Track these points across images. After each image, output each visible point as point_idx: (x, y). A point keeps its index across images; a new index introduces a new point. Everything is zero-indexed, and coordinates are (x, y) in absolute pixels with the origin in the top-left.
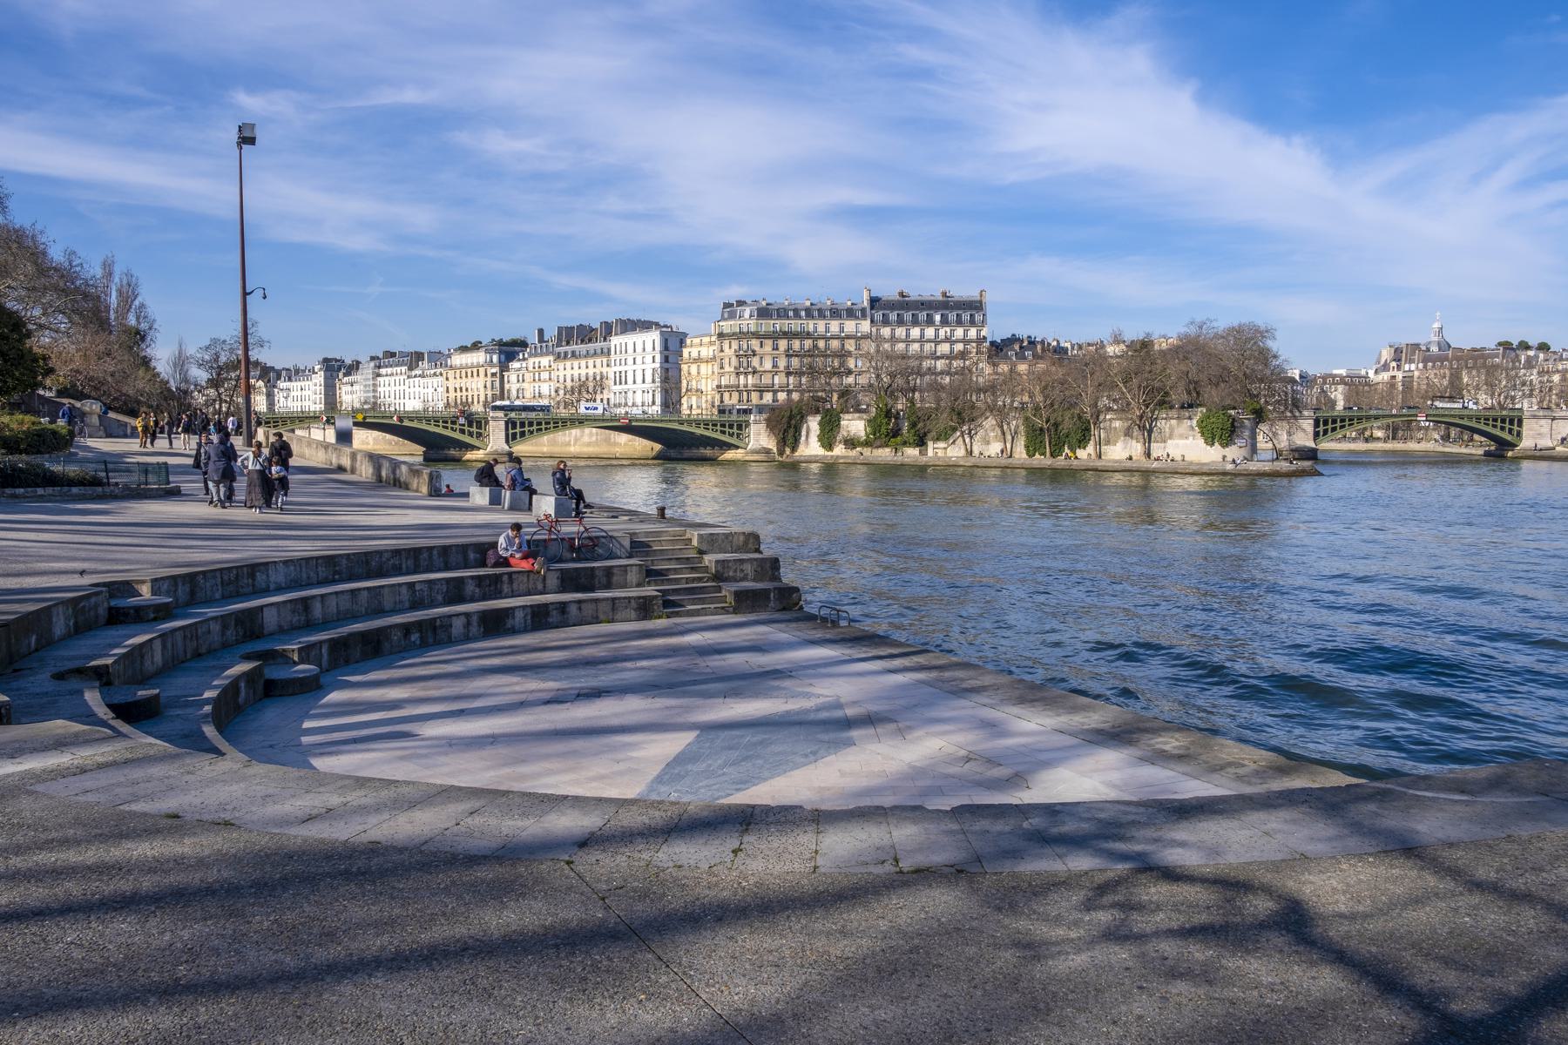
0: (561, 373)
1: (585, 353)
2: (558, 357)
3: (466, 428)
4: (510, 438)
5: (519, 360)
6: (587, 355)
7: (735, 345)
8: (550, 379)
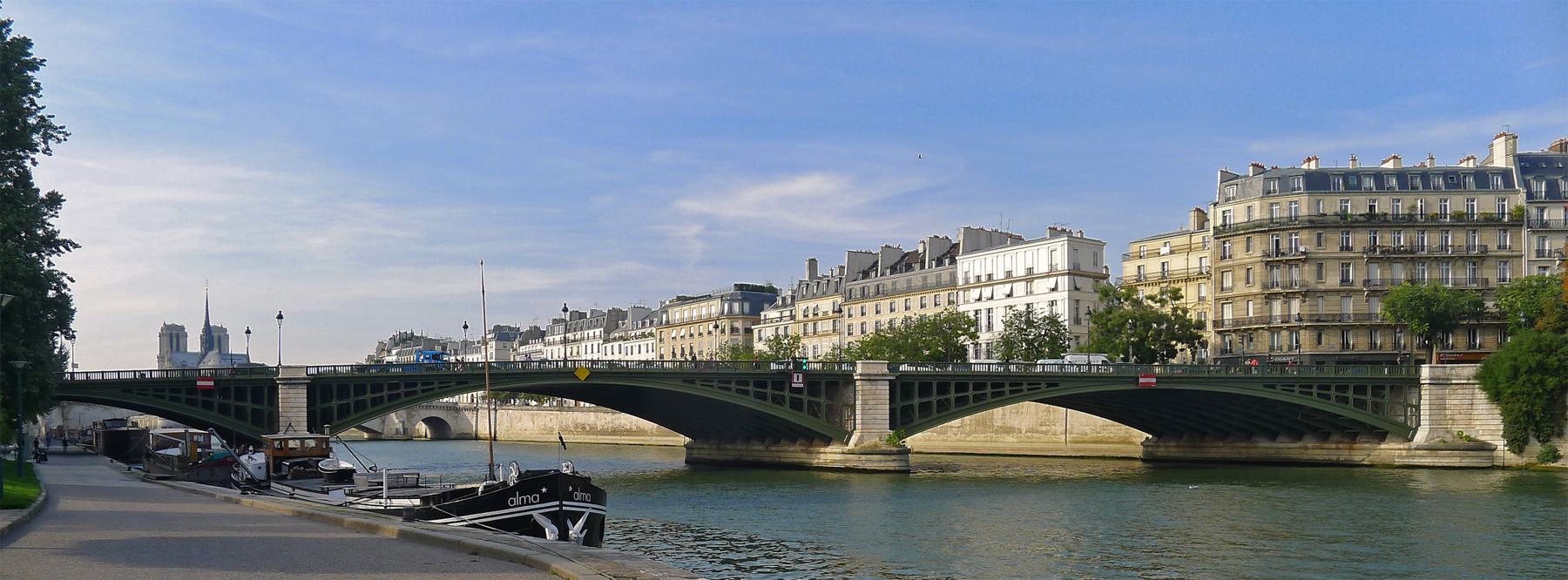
0: (856, 322)
1: (872, 290)
2: (849, 298)
3: (805, 397)
4: (904, 418)
5: (777, 307)
6: (909, 290)
7: (1260, 245)
8: (834, 331)
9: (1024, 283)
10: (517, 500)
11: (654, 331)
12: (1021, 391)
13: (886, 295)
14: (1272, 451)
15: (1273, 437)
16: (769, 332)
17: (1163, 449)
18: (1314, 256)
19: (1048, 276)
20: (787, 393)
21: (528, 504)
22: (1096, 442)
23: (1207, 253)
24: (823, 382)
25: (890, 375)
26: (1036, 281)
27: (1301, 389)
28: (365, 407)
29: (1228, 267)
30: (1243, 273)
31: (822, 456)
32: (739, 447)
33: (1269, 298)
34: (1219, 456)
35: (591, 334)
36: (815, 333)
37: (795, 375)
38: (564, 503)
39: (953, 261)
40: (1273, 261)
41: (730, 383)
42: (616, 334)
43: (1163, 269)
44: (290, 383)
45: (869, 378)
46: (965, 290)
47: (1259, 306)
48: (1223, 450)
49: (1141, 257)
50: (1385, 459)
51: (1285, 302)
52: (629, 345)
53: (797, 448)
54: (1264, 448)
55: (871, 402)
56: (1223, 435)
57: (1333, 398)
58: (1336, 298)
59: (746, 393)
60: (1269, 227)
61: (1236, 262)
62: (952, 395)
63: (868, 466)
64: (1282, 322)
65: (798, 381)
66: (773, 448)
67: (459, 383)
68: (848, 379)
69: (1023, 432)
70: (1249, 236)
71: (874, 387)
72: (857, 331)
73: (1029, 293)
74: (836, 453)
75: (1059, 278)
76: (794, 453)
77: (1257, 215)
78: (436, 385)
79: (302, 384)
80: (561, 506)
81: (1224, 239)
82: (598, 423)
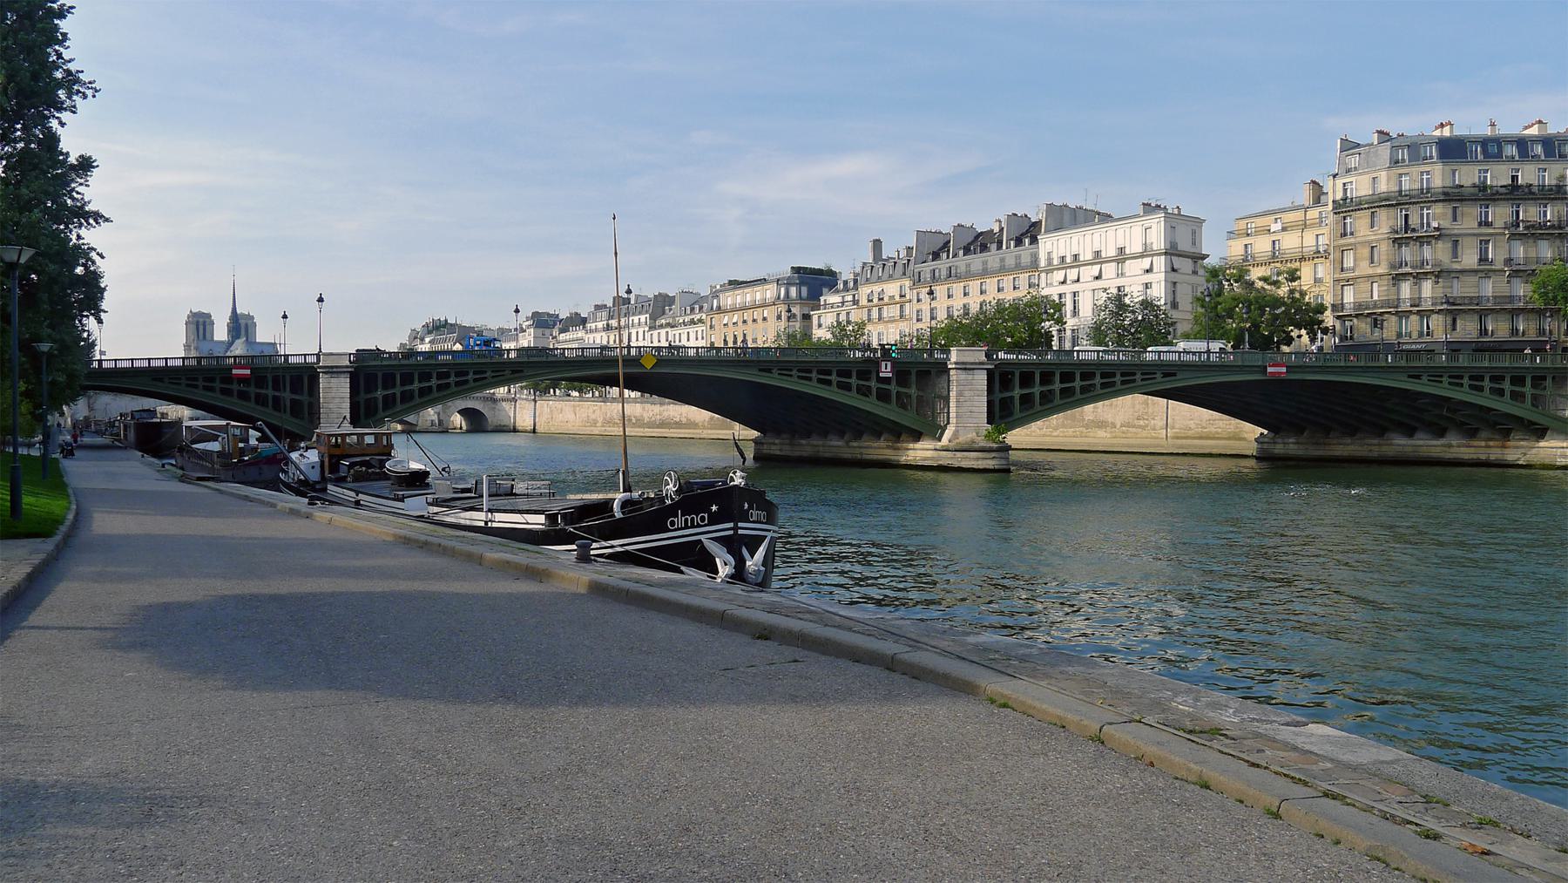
1: (944, 273)
4: (1002, 413)
5: (837, 291)
6: (985, 273)
7: (1387, 221)
8: (901, 316)
9: (1114, 264)
10: (680, 520)
11: (704, 317)
12: (1134, 381)
13: (959, 278)
14: (1410, 449)
15: (1410, 432)
16: (829, 319)
17: (1281, 446)
18: (1448, 232)
19: (1142, 256)
20: (873, 384)
21: (693, 526)
22: (1201, 438)
23: (1325, 230)
24: (914, 372)
25: (988, 364)
26: (1127, 262)
27: (1429, 378)
28: (412, 397)
29: (1348, 245)
30: (1366, 252)
31: (911, 453)
32: (815, 443)
33: (1397, 279)
34: (1346, 454)
35: (636, 321)
36: (880, 319)
37: (883, 364)
38: (740, 525)
39: (1034, 240)
40: (1403, 237)
41: (810, 372)
42: (663, 321)
43: (1274, 248)
44: (333, 371)
45: (964, 367)
46: (1047, 272)
47: (1386, 288)
48: (1351, 448)
49: (1248, 235)
50: (1543, 458)
51: (1415, 284)
52: (677, 333)
53: (882, 443)
54: (1399, 445)
55: (967, 393)
56: (1351, 431)
57: (1487, 390)
58: (1473, 279)
59: (829, 383)
60: (1398, 201)
61: (1358, 239)
62: (1057, 386)
63: (965, 464)
64: (1411, 306)
65: (886, 370)
66: (855, 444)
67: (514, 372)
68: (943, 369)
69: (1118, 427)
70: (1374, 210)
71: (970, 377)
72: (926, 316)
73: (1121, 275)
74: (928, 450)
75: (1155, 258)
76: (878, 449)
77: (1383, 187)
79: (344, 372)
80: (735, 528)
81: (1345, 214)
82: (645, 415)
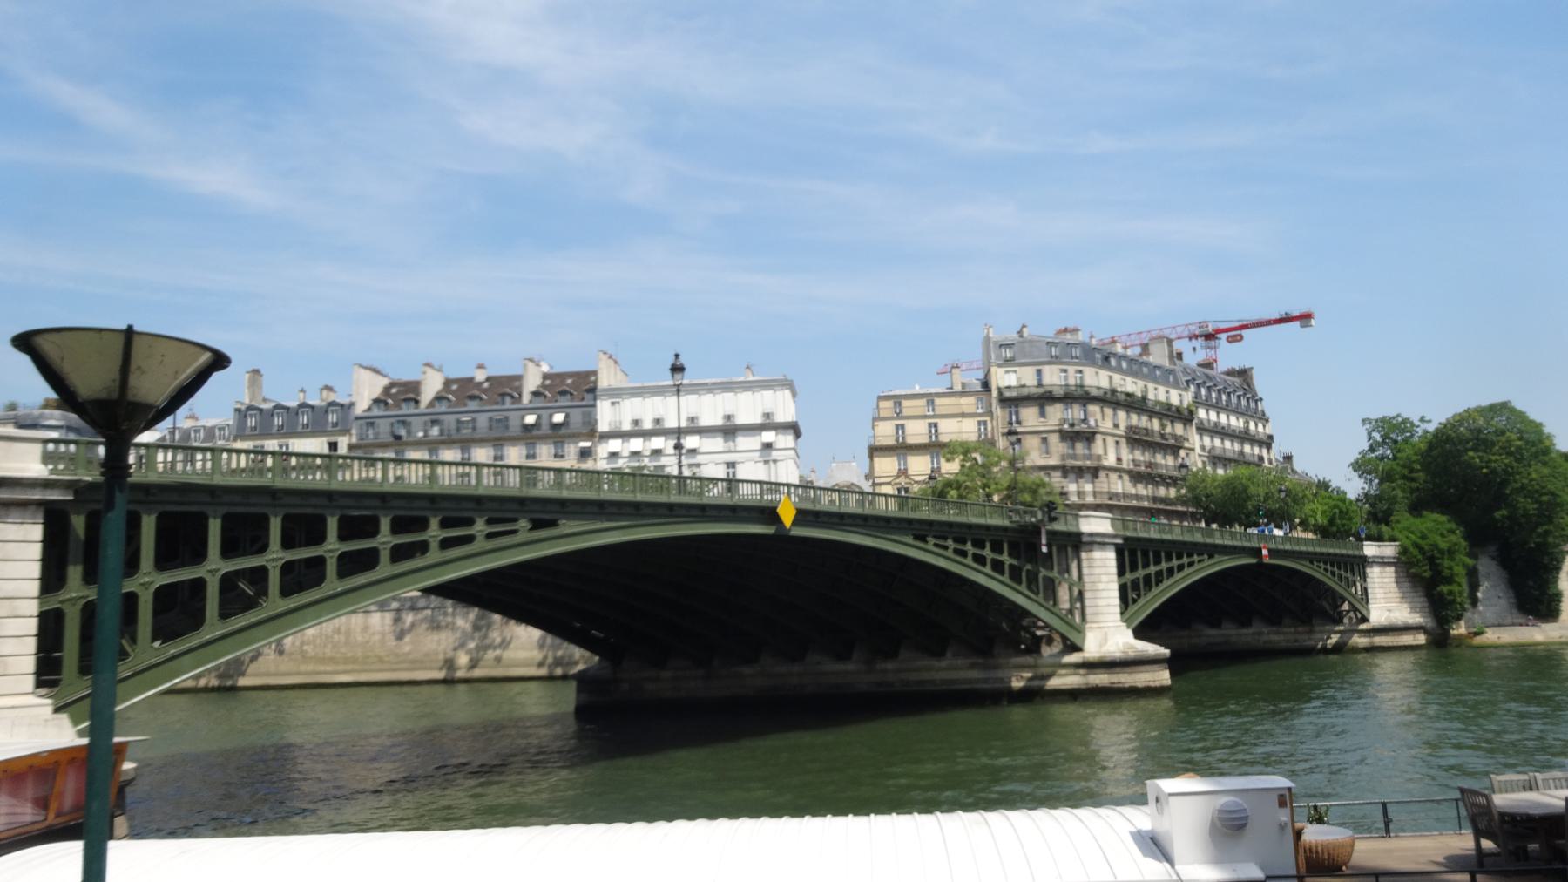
15: (1216, 624)
78: (480, 527)
79: (23, 505)
